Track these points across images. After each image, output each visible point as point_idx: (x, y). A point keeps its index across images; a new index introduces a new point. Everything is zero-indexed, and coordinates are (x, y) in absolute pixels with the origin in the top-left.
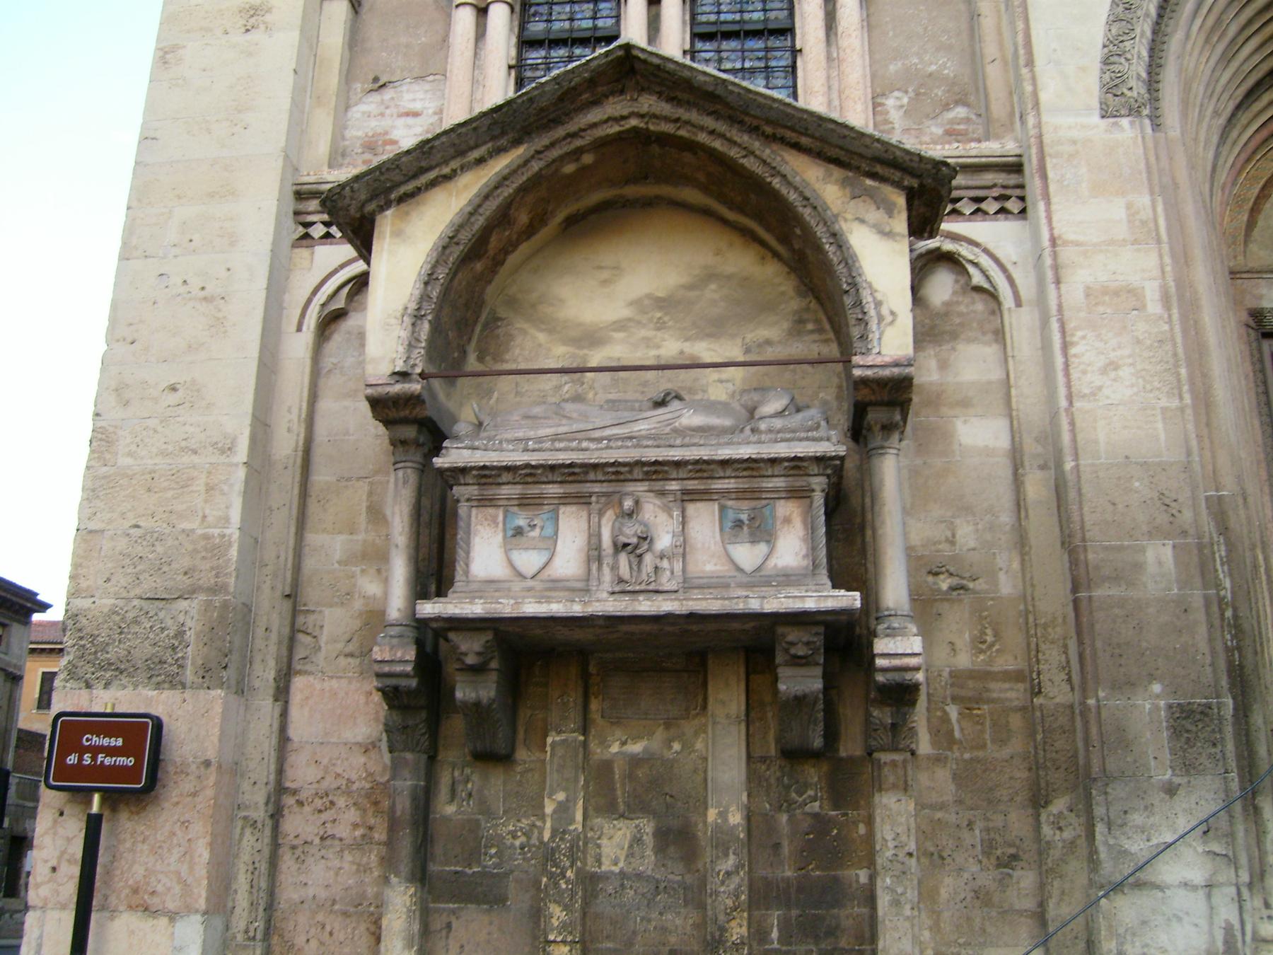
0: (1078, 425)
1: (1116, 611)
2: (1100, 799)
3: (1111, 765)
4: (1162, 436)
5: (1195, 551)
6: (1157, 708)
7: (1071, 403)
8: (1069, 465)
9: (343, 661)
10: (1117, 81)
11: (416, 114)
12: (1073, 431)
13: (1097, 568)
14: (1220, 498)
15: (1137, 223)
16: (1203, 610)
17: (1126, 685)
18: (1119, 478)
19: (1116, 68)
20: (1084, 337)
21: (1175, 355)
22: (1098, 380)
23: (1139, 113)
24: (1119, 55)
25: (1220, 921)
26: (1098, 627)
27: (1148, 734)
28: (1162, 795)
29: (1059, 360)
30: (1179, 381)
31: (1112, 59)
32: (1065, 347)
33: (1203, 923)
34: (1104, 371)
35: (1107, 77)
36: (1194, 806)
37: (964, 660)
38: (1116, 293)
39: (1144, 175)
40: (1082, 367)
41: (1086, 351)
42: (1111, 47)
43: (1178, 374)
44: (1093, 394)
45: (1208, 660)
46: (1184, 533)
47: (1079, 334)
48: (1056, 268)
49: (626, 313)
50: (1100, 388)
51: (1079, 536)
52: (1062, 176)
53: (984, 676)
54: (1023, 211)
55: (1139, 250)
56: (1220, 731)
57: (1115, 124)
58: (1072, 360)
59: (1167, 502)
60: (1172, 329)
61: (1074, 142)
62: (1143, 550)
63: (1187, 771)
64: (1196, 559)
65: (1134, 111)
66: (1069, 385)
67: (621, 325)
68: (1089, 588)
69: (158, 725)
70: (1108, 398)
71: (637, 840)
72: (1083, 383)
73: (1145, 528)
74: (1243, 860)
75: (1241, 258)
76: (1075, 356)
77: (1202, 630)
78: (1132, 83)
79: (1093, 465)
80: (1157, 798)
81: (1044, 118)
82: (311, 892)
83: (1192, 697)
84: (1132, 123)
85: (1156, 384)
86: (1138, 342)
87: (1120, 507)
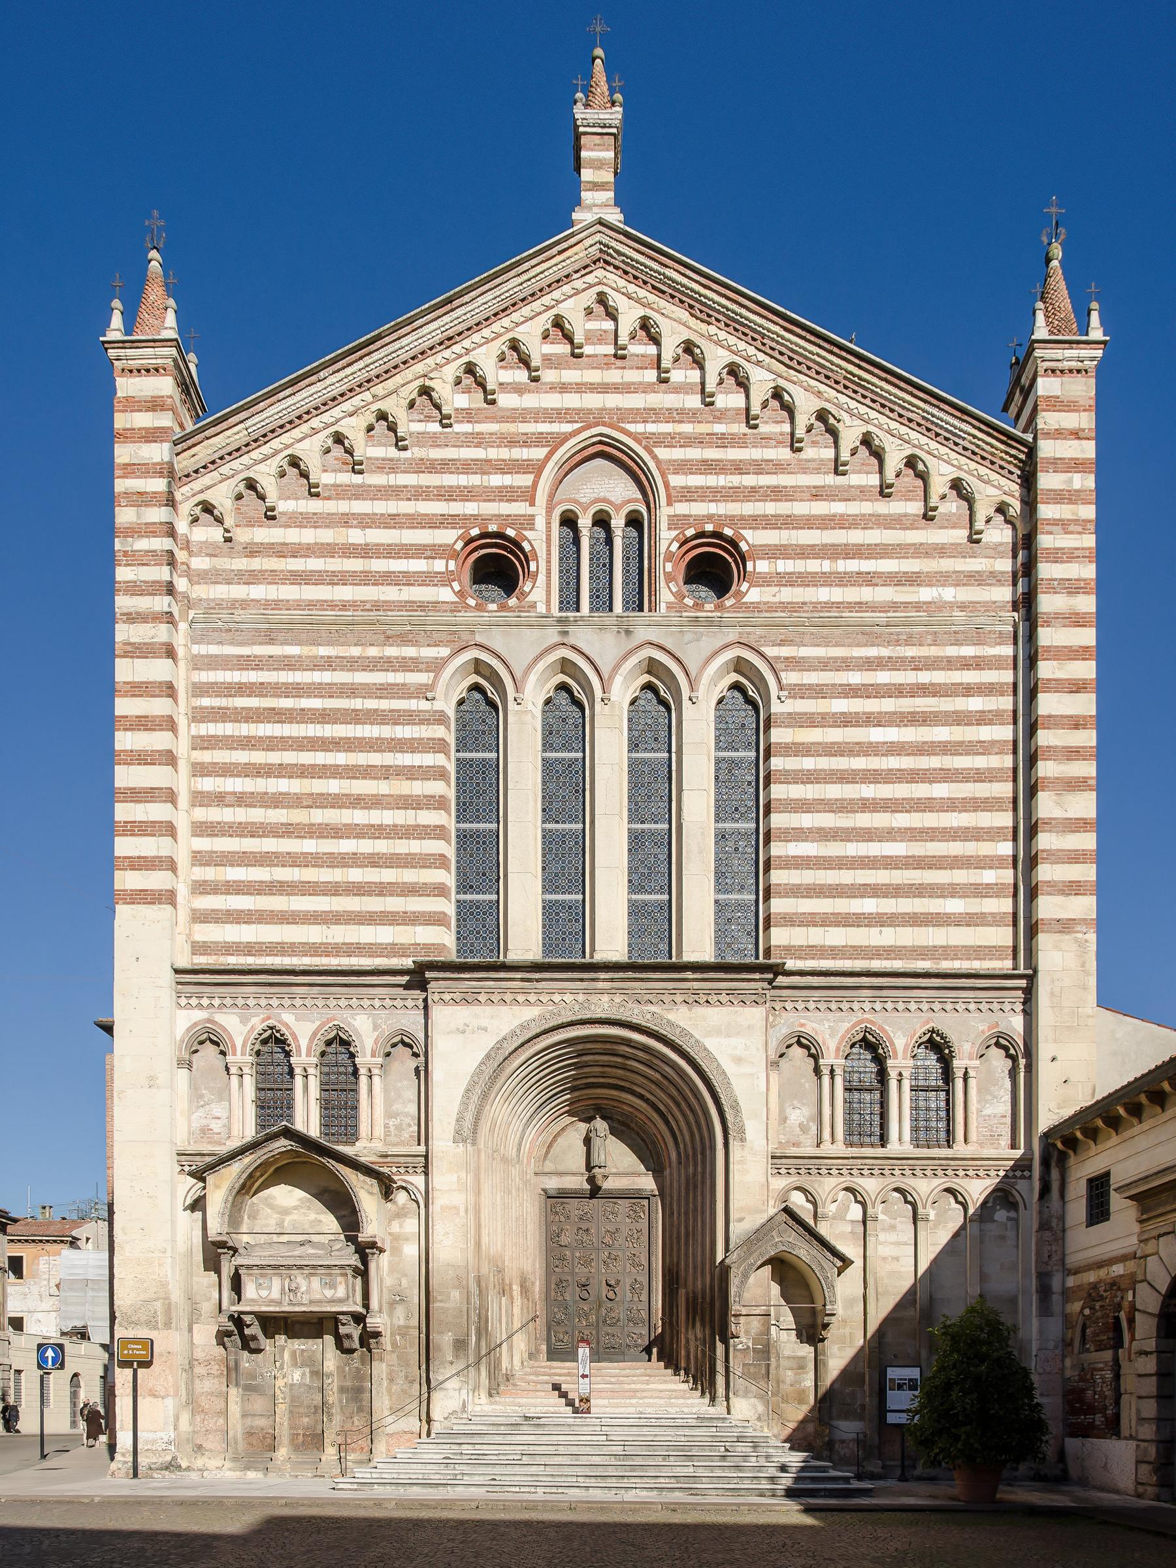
9: (210, 1319)
11: (219, 1118)
37: (402, 1322)
49: (297, 1203)
53: (407, 1327)
67: (295, 1208)
69: (152, 1341)
71: (304, 1374)
82: (205, 1390)
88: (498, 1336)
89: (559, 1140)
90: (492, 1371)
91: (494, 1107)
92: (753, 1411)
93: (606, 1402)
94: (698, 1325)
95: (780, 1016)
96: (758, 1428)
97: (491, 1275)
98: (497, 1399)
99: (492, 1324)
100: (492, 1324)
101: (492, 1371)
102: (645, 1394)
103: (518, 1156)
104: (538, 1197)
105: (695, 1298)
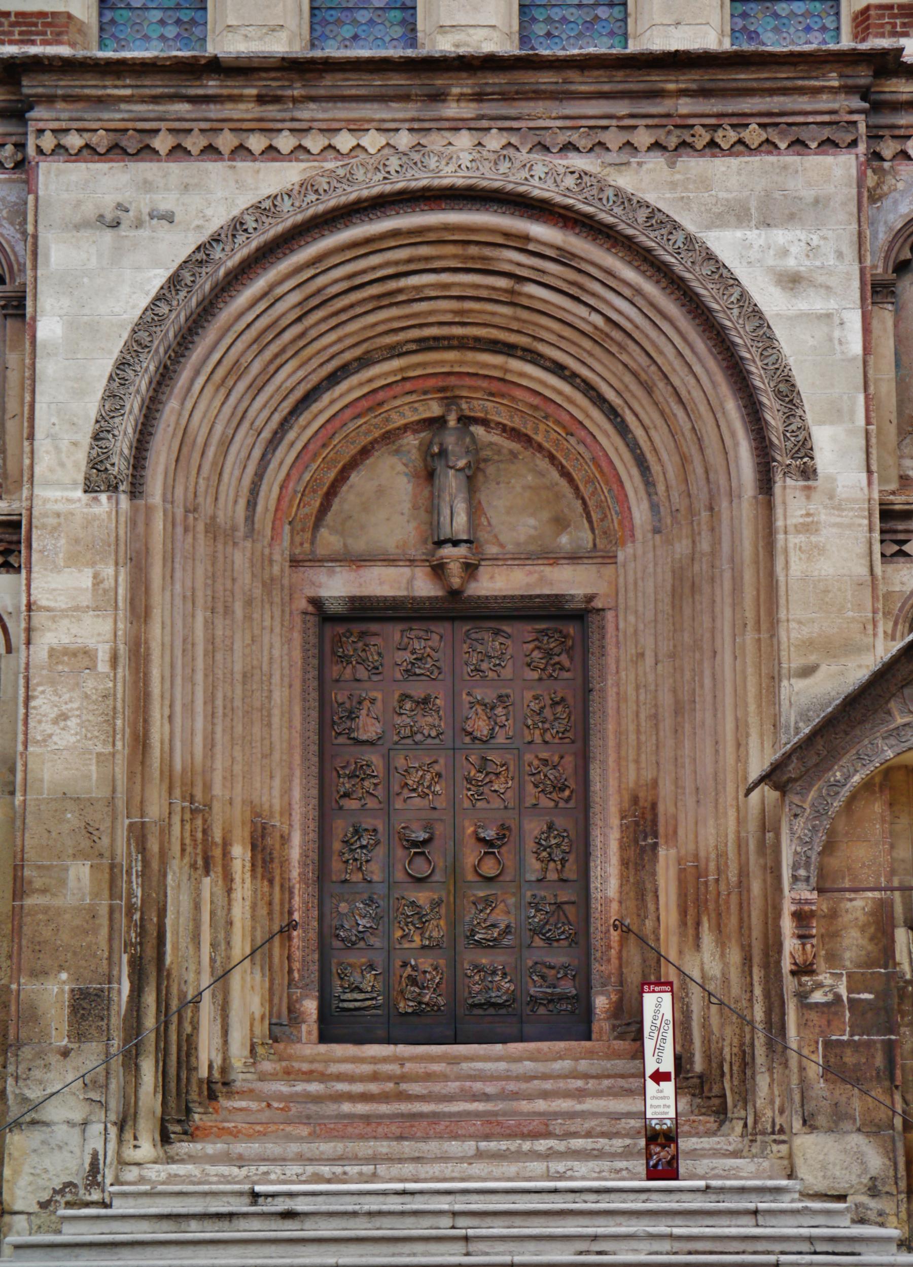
0: (29, 766)
1: (41, 916)
2: (12, 1060)
3: (23, 1035)
4: (94, 776)
5: (107, 870)
6: (63, 991)
7: (26, 748)
8: (19, 798)
10: (103, 457)
12: (25, 771)
13: (30, 882)
14: (143, 823)
15: (100, 592)
16: (107, 916)
17: (38, 974)
18: (56, 811)
19: (102, 443)
20: (43, 692)
21: (115, 708)
22: (48, 728)
23: (116, 488)
24: (108, 431)
25: (89, 1150)
26: (25, 928)
27: (53, 1012)
28: (58, 1057)
29: (22, 711)
30: (114, 730)
31: (102, 435)
32: (27, 699)
33: (77, 1151)
34: (55, 722)
35: (94, 453)
36: (80, 1064)
38: (75, 654)
39: (113, 547)
40: (38, 717)
41: (43, 703)
42: (102, 423)
43: (115, 725)
44: (44, 741)
45: (106, 954)
46: (101, 855)
47: (40, 689)
48: (29, 630)
50: (50, 736)
51: (19, 856)
52: (44, 547)
54: (20, 567)
55: (98, 616)
56: (108, 1009)
57: (96, 499)
58: (31, 711)
59: (91, 830)
60: (115, 686)
61: (58, 515)
62: (66, 869)
63: (79, 1039)
64: (107, 876)
65: (113, 488)
66: (26, 734)
68: (21, 899)
70: (56, 743)
72: (37, 730)
73: (71, 851)
74: (113, 1104)
75: (307, 546)
76: (35, 708)
77: (104, 931)
78: (115, 459)
79: (37, 799)
80: (54, 1059)
81: (37, 491)
83: (90, 983)
84: (109, 498)
85: (96, 733)
86: (87, 696)
87: (54, 834)
88: (191, 977)
89: (354, 478)
90: (172, 1071)
91: (189, 405)
92: (856, 1169)
93: (470, 1147)
94: (707, 939)
95: (893, 171)
96: (872, 1215)
97: (176, 819)
98: (184, 1147)
99: (176, 947)
100: (176, 947)
101: (172, 1071)
102: (575, 1126)
103: (250, 518)
104: (298, 620)
105: (699, 873)
